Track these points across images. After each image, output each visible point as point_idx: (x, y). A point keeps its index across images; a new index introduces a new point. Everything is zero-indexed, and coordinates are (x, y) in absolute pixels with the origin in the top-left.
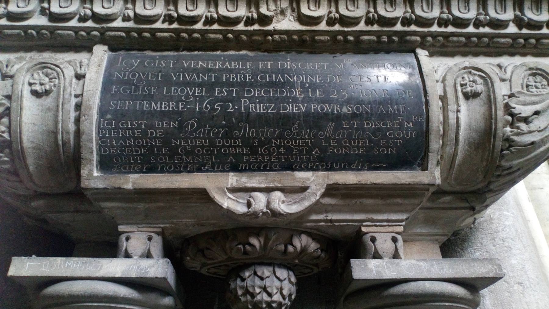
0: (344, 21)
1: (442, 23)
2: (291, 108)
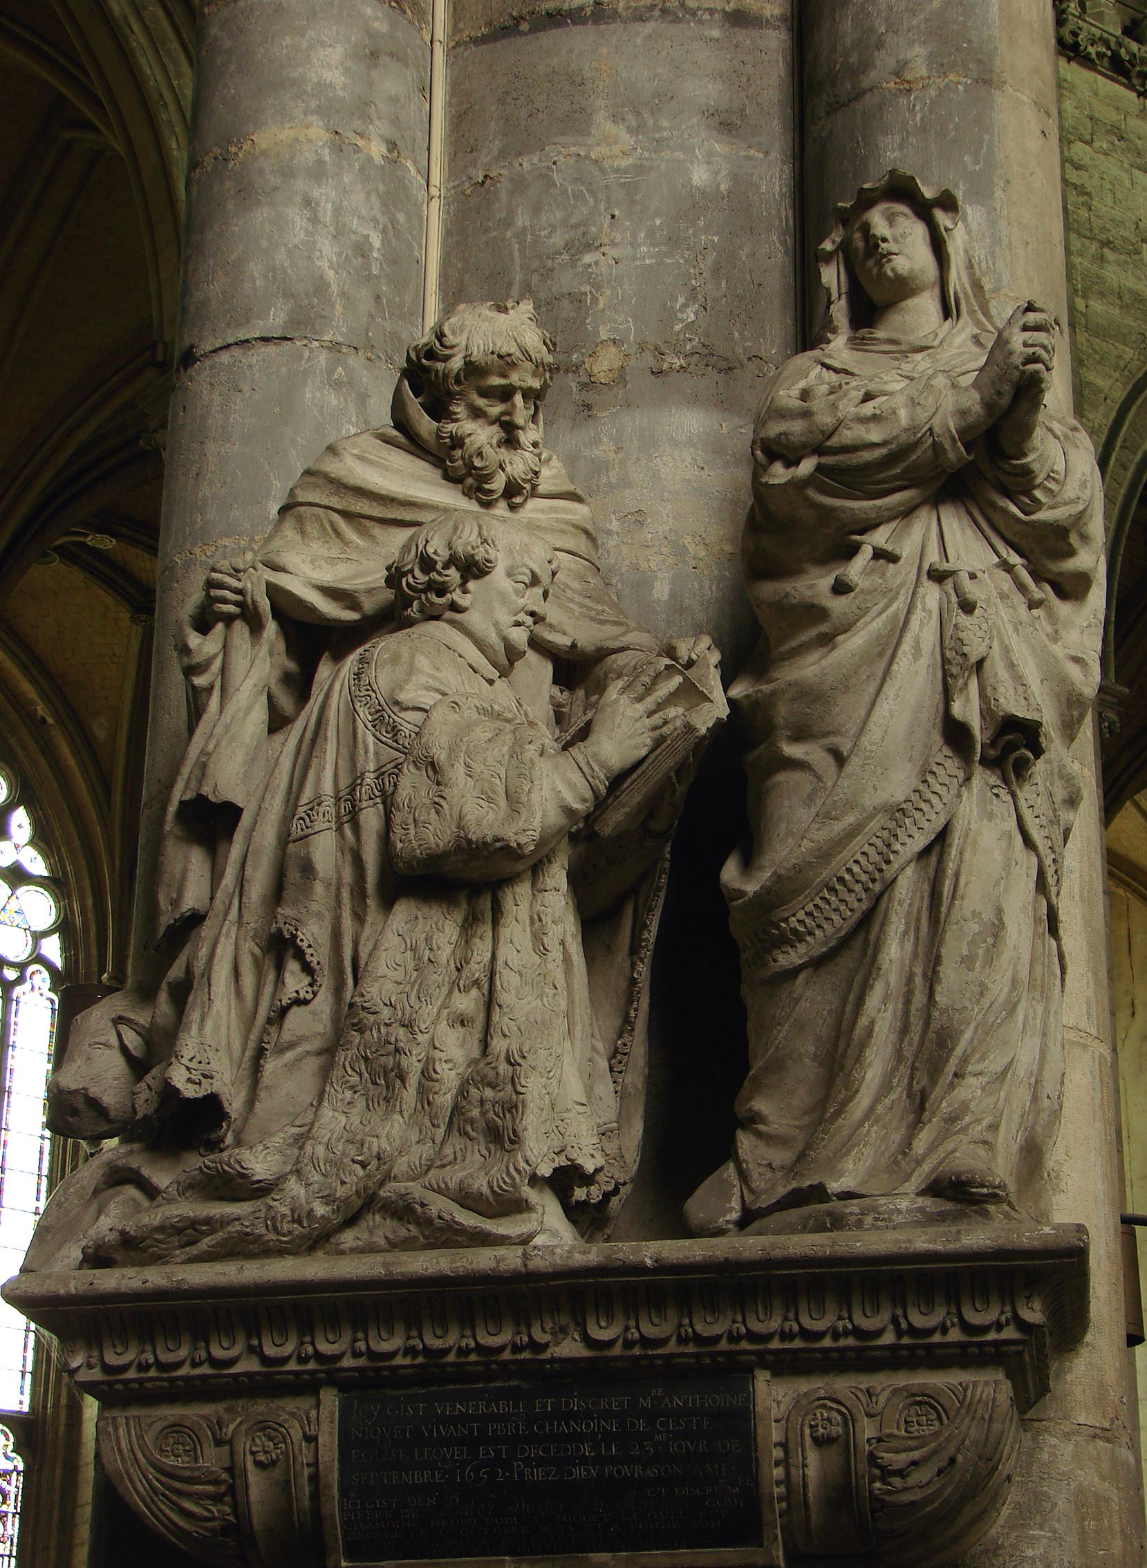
0: (645, 1342)
1: (786, 1336)
2: (578, 1473)
